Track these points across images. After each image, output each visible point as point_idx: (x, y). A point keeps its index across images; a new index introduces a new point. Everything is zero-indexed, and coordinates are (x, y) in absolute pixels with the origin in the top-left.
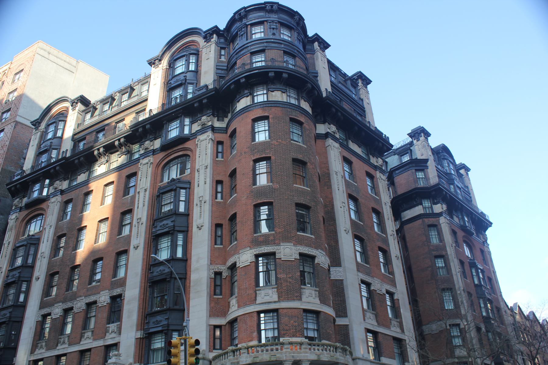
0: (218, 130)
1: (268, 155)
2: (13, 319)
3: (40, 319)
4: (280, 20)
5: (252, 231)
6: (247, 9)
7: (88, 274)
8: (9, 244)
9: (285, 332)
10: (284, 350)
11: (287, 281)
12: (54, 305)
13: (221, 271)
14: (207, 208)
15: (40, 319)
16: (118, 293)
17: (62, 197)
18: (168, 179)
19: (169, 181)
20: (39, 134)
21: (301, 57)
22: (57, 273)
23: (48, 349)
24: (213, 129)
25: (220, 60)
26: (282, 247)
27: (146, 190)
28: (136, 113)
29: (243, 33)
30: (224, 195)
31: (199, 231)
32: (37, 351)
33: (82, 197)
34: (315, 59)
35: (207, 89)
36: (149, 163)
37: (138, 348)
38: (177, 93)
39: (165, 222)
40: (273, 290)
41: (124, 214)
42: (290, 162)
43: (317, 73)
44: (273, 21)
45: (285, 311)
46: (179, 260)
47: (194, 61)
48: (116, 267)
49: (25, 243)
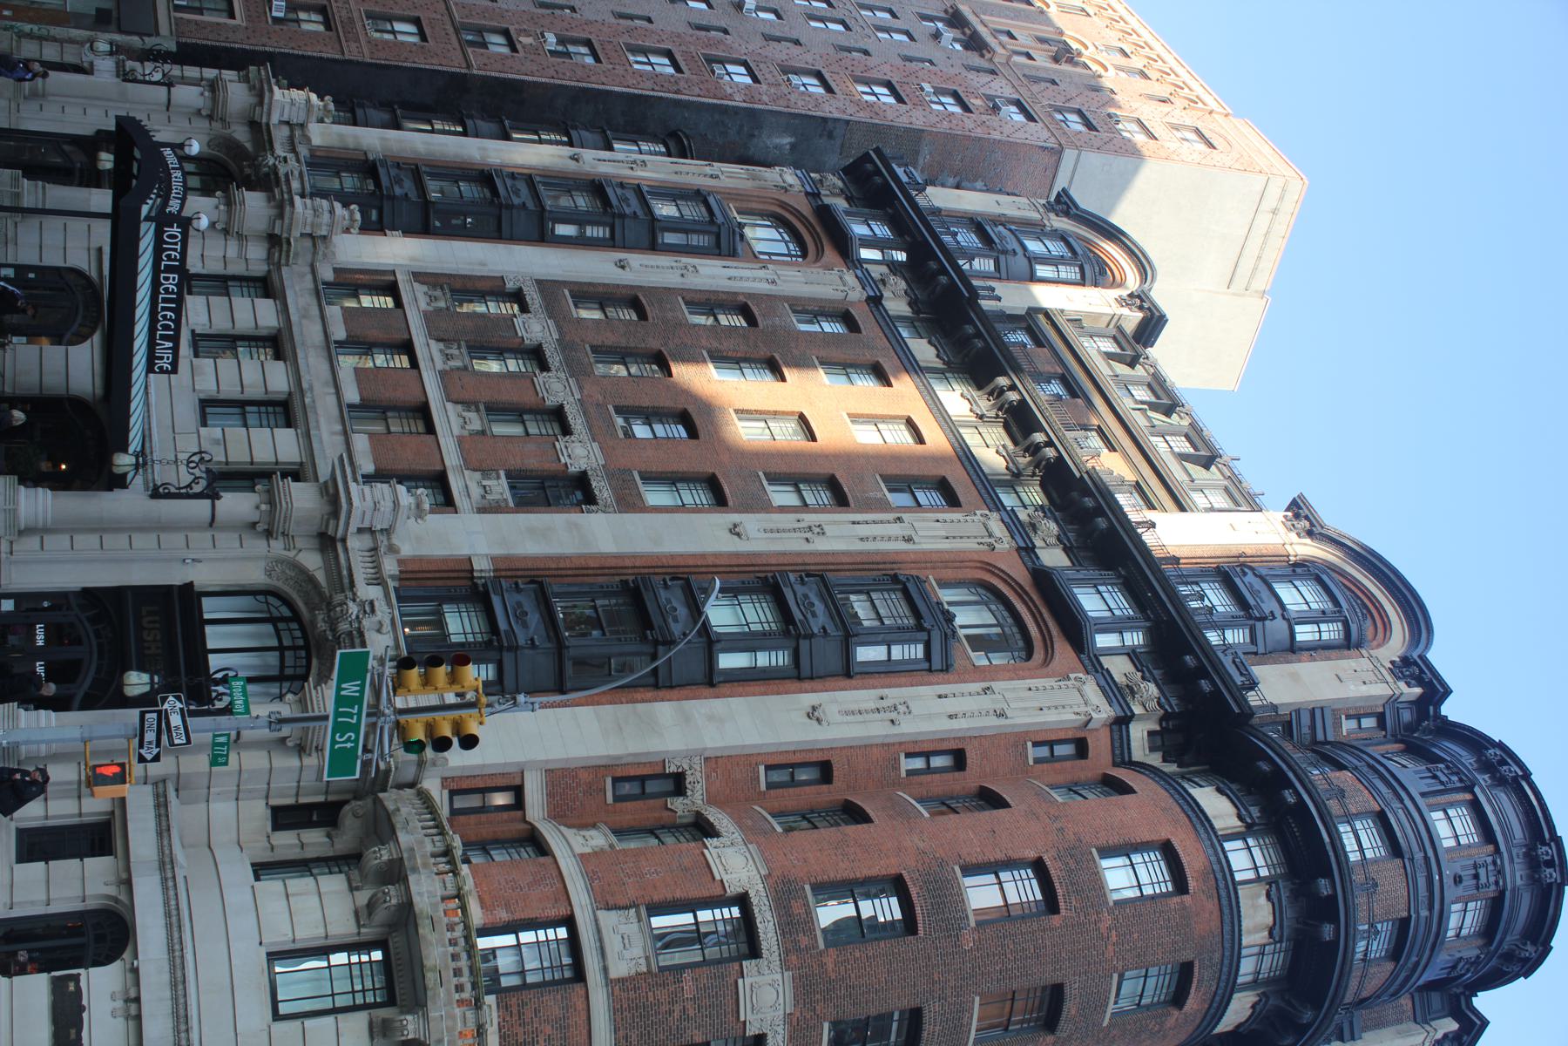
0: (1121, 738)
1: (1062, 905)
2: (505, 214)
3: (510, 285)
4: (1508, 894)
5: (819, 878)
6: (1524, 784)
7: (646, 402)
8: (711, 176)
9: (515, 1011)
10: (458, 1011)
11: (673, 1002)
12: (550, 318)
13: (689, 793)
14: (876, 730)
15: (510, 285)
16: (597, 493)
17: (859, 301)
18: (950, 603)
19: (946, 607)
20: (1035, 216)
21: (1398, 975)
22: (642, 315)
23: (429, 318)
24: (1122, 722)
25: (1343, 717)
26: (779, 976)
27: (909, 540)
28: (1137, 482)
29: (1444, 779)
30: (923, 778)
31: (803, 713)
32: (420, 289)
33: (869, 357)
34: (1399, 1027)
35: (1244, 689)
36: (992, 540)
37: (444, 568)
38: (1217, 598)
39: (819, 607)
40: (643, 961)
41: (833, 485)
42: (1049, 977)
43: (1353, 1038)
44: (1500, 872)
45: (580, 1005)
46: (711, 661)
47: (1325, 636)
48: (671, 479)
49: (720, 219)
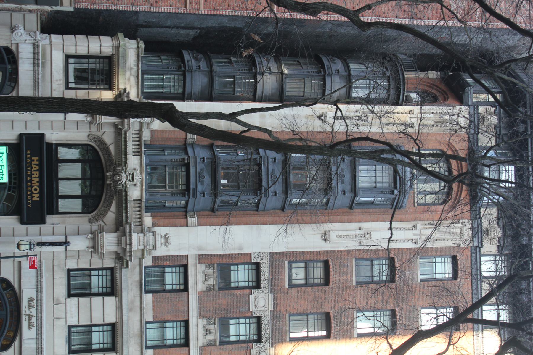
15: (254, 260)
23: (202, 297)
32: (201, 268)
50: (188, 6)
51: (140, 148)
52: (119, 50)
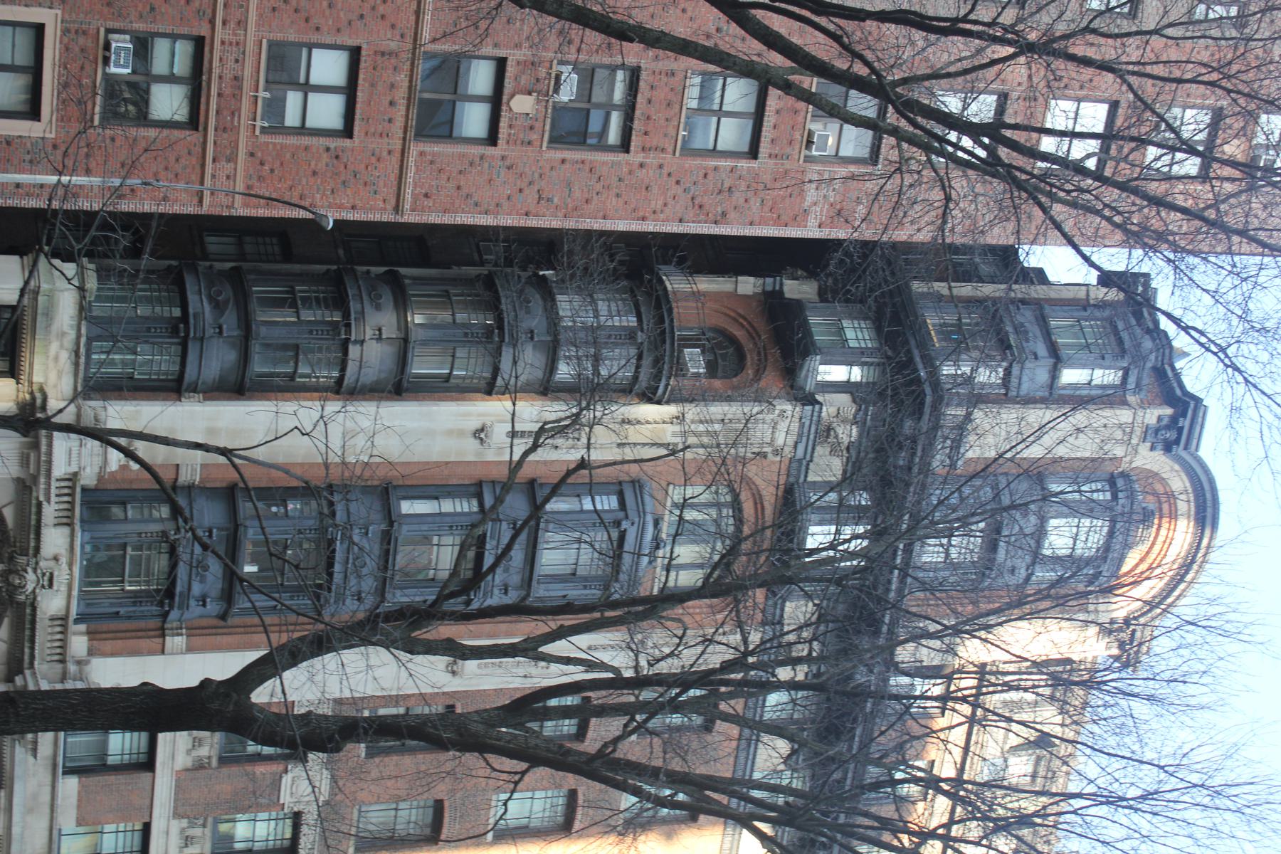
50: (207, 199)
51: (72, 510)
52: (36, 299)
